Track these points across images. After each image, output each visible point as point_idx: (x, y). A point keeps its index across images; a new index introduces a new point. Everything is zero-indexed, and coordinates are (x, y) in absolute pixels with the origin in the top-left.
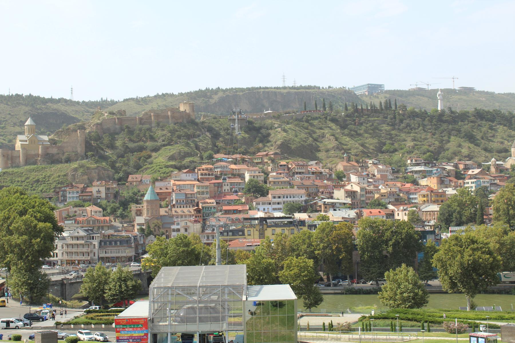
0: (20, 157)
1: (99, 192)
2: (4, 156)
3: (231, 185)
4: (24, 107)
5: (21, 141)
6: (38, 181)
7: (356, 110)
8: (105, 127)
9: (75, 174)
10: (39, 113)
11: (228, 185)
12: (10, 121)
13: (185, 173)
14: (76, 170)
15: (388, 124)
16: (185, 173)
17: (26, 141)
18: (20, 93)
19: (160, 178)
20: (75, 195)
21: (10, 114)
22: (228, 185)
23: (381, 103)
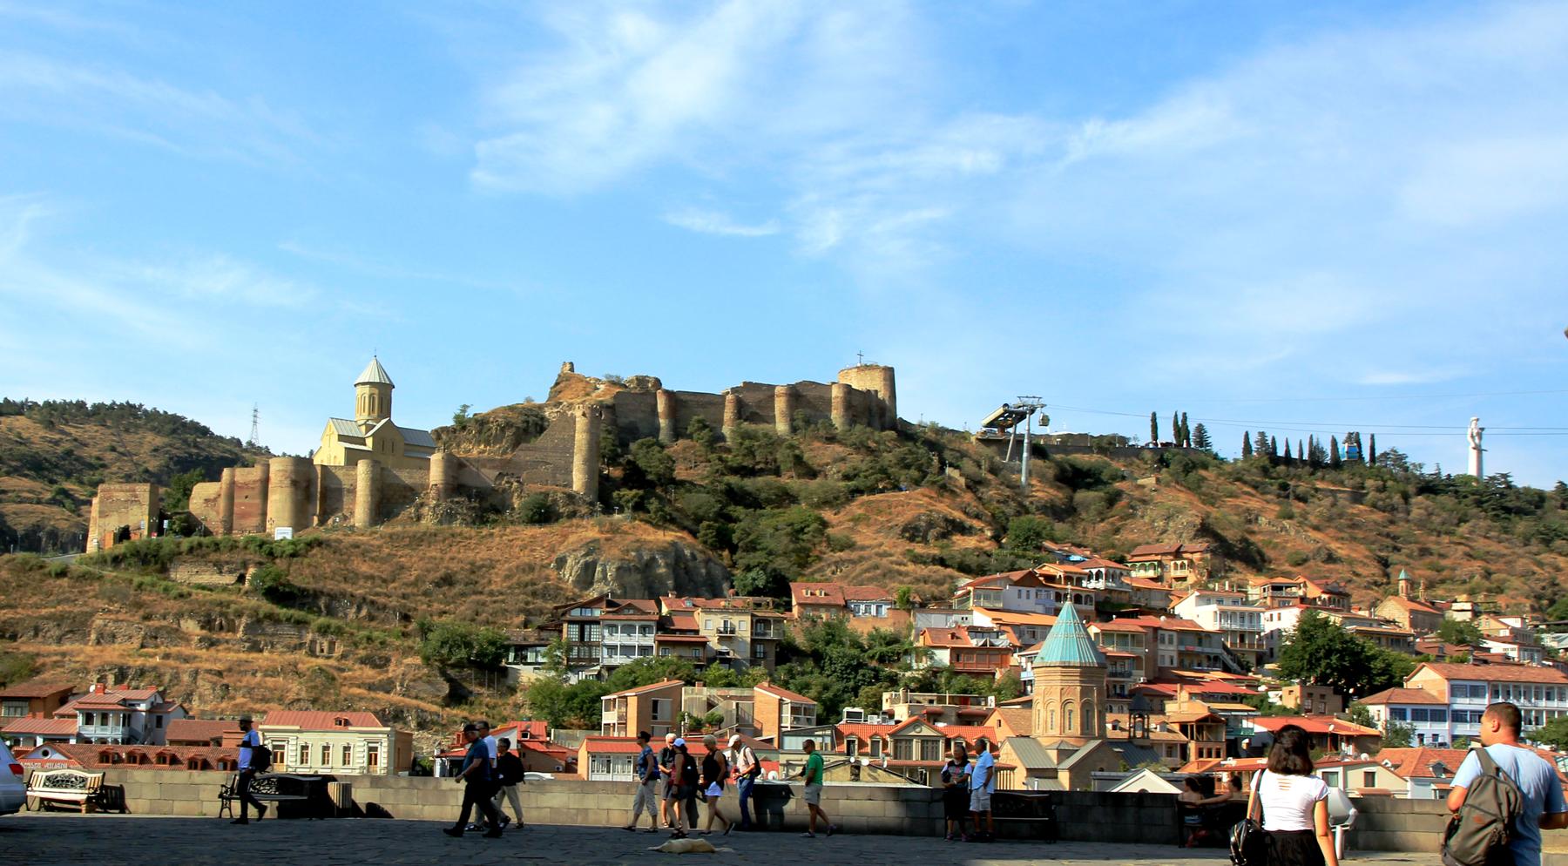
0: (353, 491)
1: (727, 636)
2: (294, 483)
3: (1181, 642)
4: (150, 437)
5: (342, 438)
6: (448, 580)
7: (1275, 460)
8: (623, 421)
9: (594, 563)
10: (191, 455)
11: (1171, 642)
12: (114, 469)
13: (1017, 583)
14: (592, 548)
15: (1374, 506)
16: (1017, 583)
17: (362, 441)
18: (135, 401)
19: (918, 599)
20: (637, 639)
21: (113, 449)
22: (1171, 642)
23: (1334, 443)
